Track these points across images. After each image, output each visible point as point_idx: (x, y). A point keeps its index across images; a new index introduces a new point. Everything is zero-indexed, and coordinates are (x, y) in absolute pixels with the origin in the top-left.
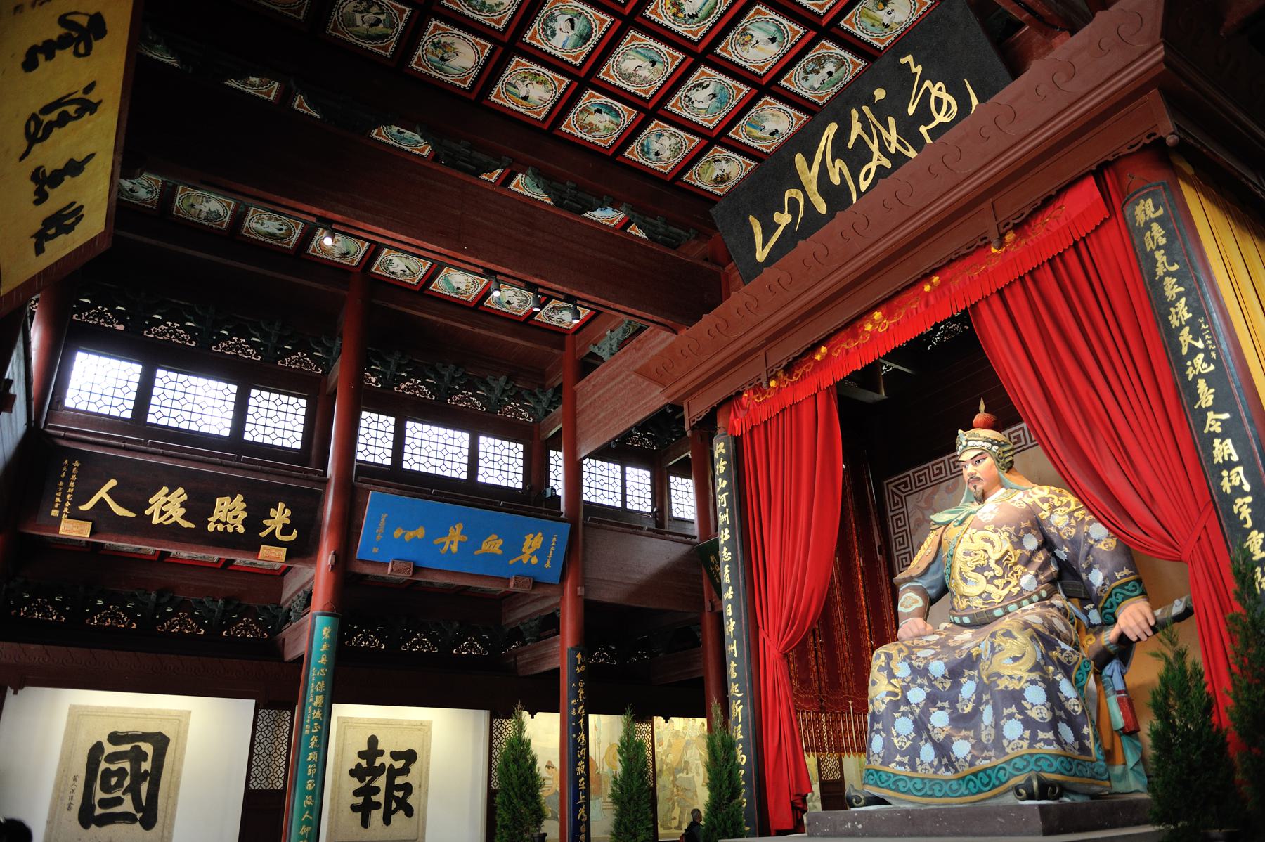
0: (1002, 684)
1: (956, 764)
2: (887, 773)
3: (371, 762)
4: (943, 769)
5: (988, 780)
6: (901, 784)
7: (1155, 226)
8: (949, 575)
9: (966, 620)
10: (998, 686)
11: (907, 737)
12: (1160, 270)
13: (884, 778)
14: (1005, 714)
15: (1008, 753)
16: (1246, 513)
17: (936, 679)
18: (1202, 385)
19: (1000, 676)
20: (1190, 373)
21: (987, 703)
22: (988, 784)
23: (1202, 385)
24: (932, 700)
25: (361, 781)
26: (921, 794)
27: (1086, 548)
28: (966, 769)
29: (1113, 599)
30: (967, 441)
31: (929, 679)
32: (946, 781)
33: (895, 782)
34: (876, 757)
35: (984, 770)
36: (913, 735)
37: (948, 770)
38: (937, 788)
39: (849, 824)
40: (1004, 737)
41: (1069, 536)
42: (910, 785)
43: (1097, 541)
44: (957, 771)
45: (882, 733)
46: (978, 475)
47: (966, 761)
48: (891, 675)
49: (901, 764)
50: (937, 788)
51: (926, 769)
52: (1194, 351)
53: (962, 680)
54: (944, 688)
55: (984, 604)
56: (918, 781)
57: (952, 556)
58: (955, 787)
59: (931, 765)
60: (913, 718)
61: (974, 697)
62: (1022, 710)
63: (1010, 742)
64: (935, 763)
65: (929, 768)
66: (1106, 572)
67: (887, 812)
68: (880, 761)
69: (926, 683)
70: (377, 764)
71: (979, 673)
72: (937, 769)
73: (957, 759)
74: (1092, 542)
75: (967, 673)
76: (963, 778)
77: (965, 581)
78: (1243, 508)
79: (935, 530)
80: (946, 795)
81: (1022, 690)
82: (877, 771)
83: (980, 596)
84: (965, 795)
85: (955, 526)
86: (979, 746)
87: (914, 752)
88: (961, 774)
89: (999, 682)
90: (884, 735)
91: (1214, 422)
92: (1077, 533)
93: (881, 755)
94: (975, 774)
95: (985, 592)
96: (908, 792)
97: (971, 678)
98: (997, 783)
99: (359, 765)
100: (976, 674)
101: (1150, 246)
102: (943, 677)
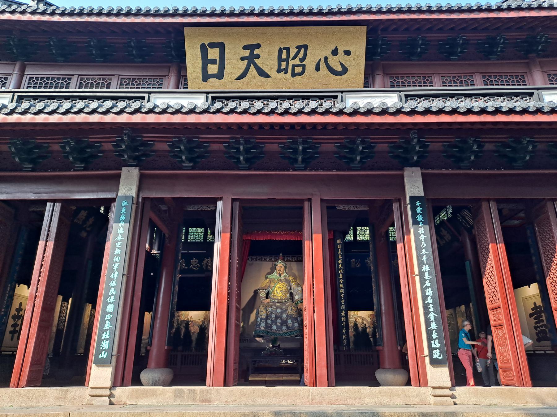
0: (294, 316)
3: (18, 313)
6: (269, 334)
7: (340, 245)
9: (276, 301)
12: (339, 253)
16: (343, 296)
18: (341, 274)
19: (293, 315)
20: (340, 272)
23: (341, 274)
24: (276, 317)
25: (14, 321)
28: (286, 331)
29: (298, 302)
32: (279, 333)
33: (267, 333)
35: (290, 332)
37: (279, 331)
38: (286, 334)
42: (271, 334)
44: (282, 331)
48: (267, 311)
49: (268, 329)
50: (277, 335)
52: (341, 269)
59: (275, 330)
62: (297, 321)
70: (20, 315)
71: (287, 314)
72: (277, 331)
76: (284, 333)
77: (277, 293)
78: (342, 296)
81: (297, 318)
82: (263, 330)
86: (288, 328)
87: (271, 327)
88: (284, 332)
91: (341, 281)
94: (287, 332)
99: (15, 314)
101: (338, 248)
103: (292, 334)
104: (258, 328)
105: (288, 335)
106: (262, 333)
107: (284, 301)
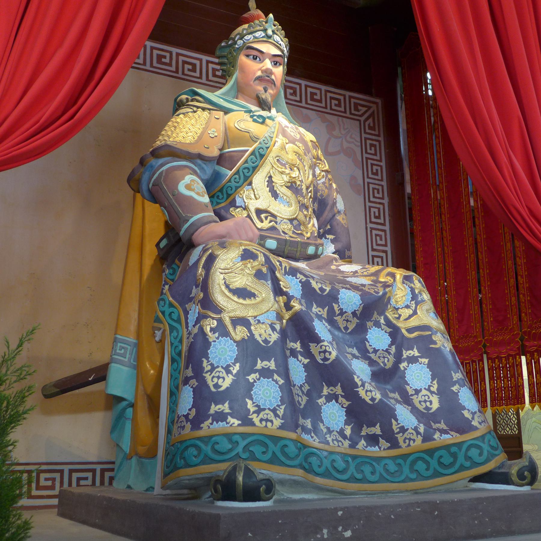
1: (399, 436)
2: (295, 441)
4: (363, 442)
5: (452, 460)
8: (246, 178)
10: (435, 343)
11: (301, 387)
13: (292, 450)
14: (455, 379)
15: (476, 428)
17: (342, 313)
21: (412, 360)
22: (452, 465)
26: (345, 477)
27: (330, 215)
30: (273, 31)
31: (331, 312)
32: (379, 459)
34: (271, 416)
35: (447, 447)
36: (307, 387)
37: (373, 440)
39: (325, 531)
40: (464, 408)
41: (322, 195)
43: (339, 212)
44: (395, 444)
45: (276, 377)
46: (273, 77)
47: (418, 433)
48: (278, 291)
50: (367, 469)
51: (336, 440)
53: (369, 324)
54: (346, 328)
55: (294, 232)
56: (338, 458)
57: (262, 156)
58: (392, 467)
59: (341, 433)
60: (306, 361)
61: (393, 349)
63: (474, 414)
64: (348, 431)
65: (340, 439)
66: (340, 246)
67: (400, 505)
68: (278, 422)
69: (325, 316)
73: (403, 430)
74: (336, 211)
75: (375, 315)
76: (404, 457)
77: (275, 195)
79: (204, 109)
80: (382, 479)
82: (275, 439)
83: (291, 220)
84: (412, 480)
85: (255, 121)
88: (404, 449)
89: (434, 338)
90: (281, 382)
92: (328, 195)
93: (281, 412)
94: (431, 452)
95: (296, 219)
96: (326, 474)
97: (377, 324)
98: (468, 464)
100: (382, 321)
102: (354, 314)
103: (461, 459)
104: (221, 417)
105: (437, 474)
106: (274, 461)
107: (311, 250)
